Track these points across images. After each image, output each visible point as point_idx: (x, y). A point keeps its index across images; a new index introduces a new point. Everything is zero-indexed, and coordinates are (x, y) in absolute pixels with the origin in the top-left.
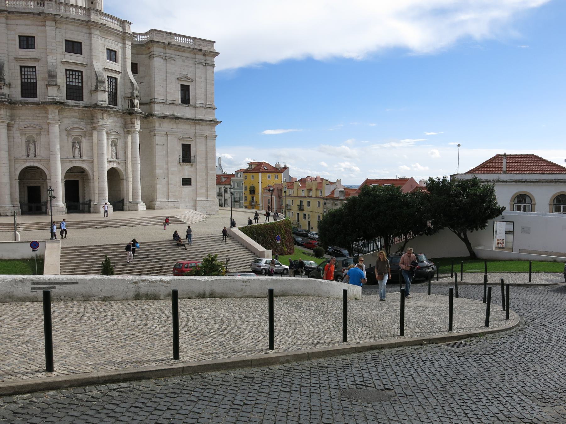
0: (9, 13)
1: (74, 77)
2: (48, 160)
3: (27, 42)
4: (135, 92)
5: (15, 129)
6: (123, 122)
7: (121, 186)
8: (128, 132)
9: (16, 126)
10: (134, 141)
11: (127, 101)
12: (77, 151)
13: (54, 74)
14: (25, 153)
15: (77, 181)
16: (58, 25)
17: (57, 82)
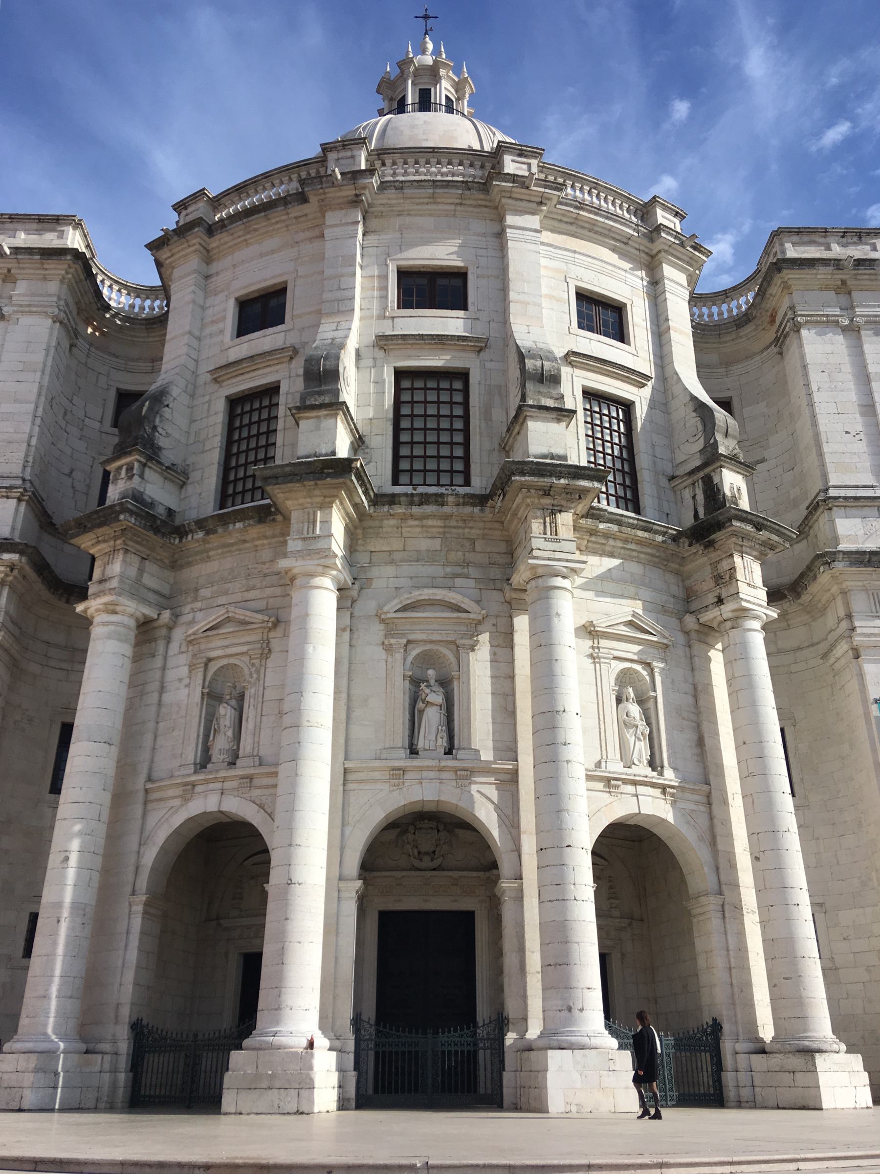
0: (211, 230)
1: (432, 397)
2: (273, 773)
3: (261, 310)
4: (719, 437)
5: (174, 648)
6: (674, 589)
7: (700, 944)
8: (707, 633)
9: (178, 634)
10: (743, 677)
11: (687, 494)
12: (432, 717)
13: (330, 364)
14: (191, 754)
15: (469, 916)
16: (374, 223)
17: (337, 393)
